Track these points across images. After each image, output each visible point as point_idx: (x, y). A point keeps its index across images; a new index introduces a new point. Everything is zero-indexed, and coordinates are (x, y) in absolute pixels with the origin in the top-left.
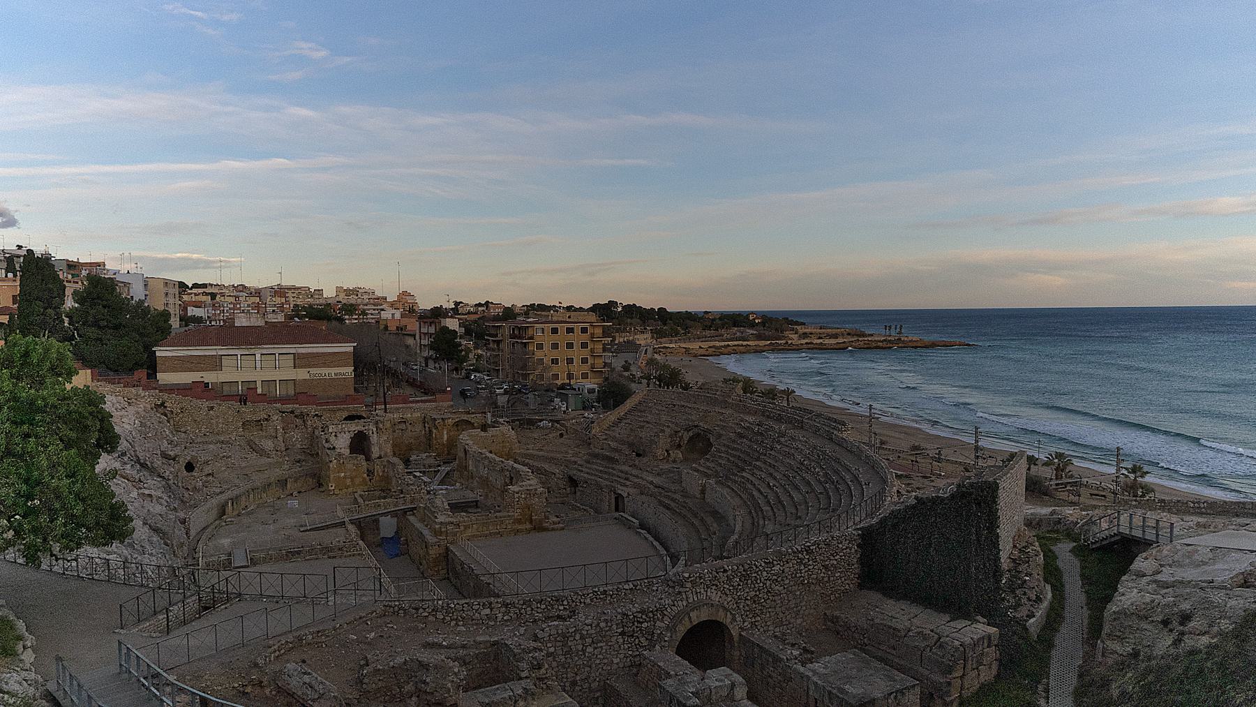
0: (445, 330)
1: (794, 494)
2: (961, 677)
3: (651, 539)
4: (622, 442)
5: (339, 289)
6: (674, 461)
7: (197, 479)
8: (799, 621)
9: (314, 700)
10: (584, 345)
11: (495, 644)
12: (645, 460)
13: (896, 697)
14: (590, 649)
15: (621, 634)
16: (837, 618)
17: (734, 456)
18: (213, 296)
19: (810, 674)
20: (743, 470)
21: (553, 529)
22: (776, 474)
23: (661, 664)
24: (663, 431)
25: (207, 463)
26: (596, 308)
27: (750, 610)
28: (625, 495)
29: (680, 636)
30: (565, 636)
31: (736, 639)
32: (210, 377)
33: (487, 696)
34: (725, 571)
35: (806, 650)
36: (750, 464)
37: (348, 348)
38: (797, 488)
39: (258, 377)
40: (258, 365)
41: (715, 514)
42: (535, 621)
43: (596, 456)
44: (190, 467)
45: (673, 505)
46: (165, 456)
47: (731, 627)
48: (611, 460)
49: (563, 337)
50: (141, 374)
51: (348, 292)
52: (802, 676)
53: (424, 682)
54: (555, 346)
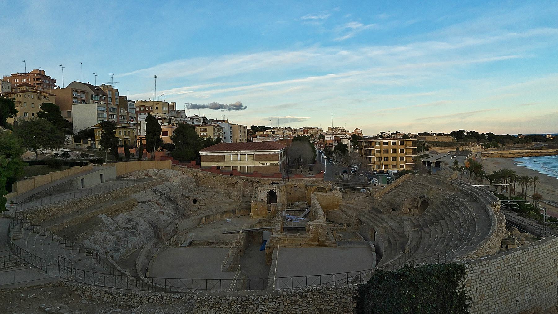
7: (196, 207)
10: (402, 151)
12: (395, 213)
18: (273, 132)
21: (330, 247)
24: (407, 198)
25: (202, 200)
26: (453, 134)
32: (220, 164)
39: (239, 164)
40: (239, 159)
43: (374, 209)
44: (195, 201)
48: (379, 212)
49: (389, 147)
50: (193, 162)
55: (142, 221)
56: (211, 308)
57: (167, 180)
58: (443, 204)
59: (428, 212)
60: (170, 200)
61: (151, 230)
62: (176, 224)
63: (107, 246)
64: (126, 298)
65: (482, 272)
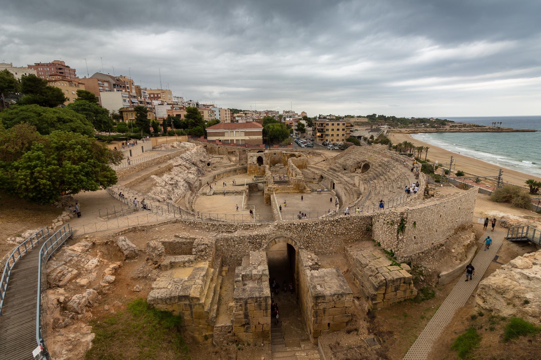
2: (384, 294)
4: (340, 164)
5: (284, 111)
6: (357, 173)
8: (331, 248)
10: (343, 130)
12: (346, 171)
13: (338, 297)
14: (237, 246)
15: (249, 242)
18: (246, 114)
20: (375, 179)
25: (214, 163)
26: (368, 117)
30: (227, 240)
32: (221, 138)
39: (235, 138)
43: (331, 169)
44: (209, 164)
46: (201, 161)
47: (294, 247)
49: (335, 127)
50: (202, 137)
51: (287, 112)
54: (333, 130)
55: (179, 179)
56: (285, 230)
57: (188, 150)
58: (380, 166)
59: (370, 171)
60: (194, 164)
61: (186, 185)
62: (200, 180)
63: (164, 196)
65: (444, 206)
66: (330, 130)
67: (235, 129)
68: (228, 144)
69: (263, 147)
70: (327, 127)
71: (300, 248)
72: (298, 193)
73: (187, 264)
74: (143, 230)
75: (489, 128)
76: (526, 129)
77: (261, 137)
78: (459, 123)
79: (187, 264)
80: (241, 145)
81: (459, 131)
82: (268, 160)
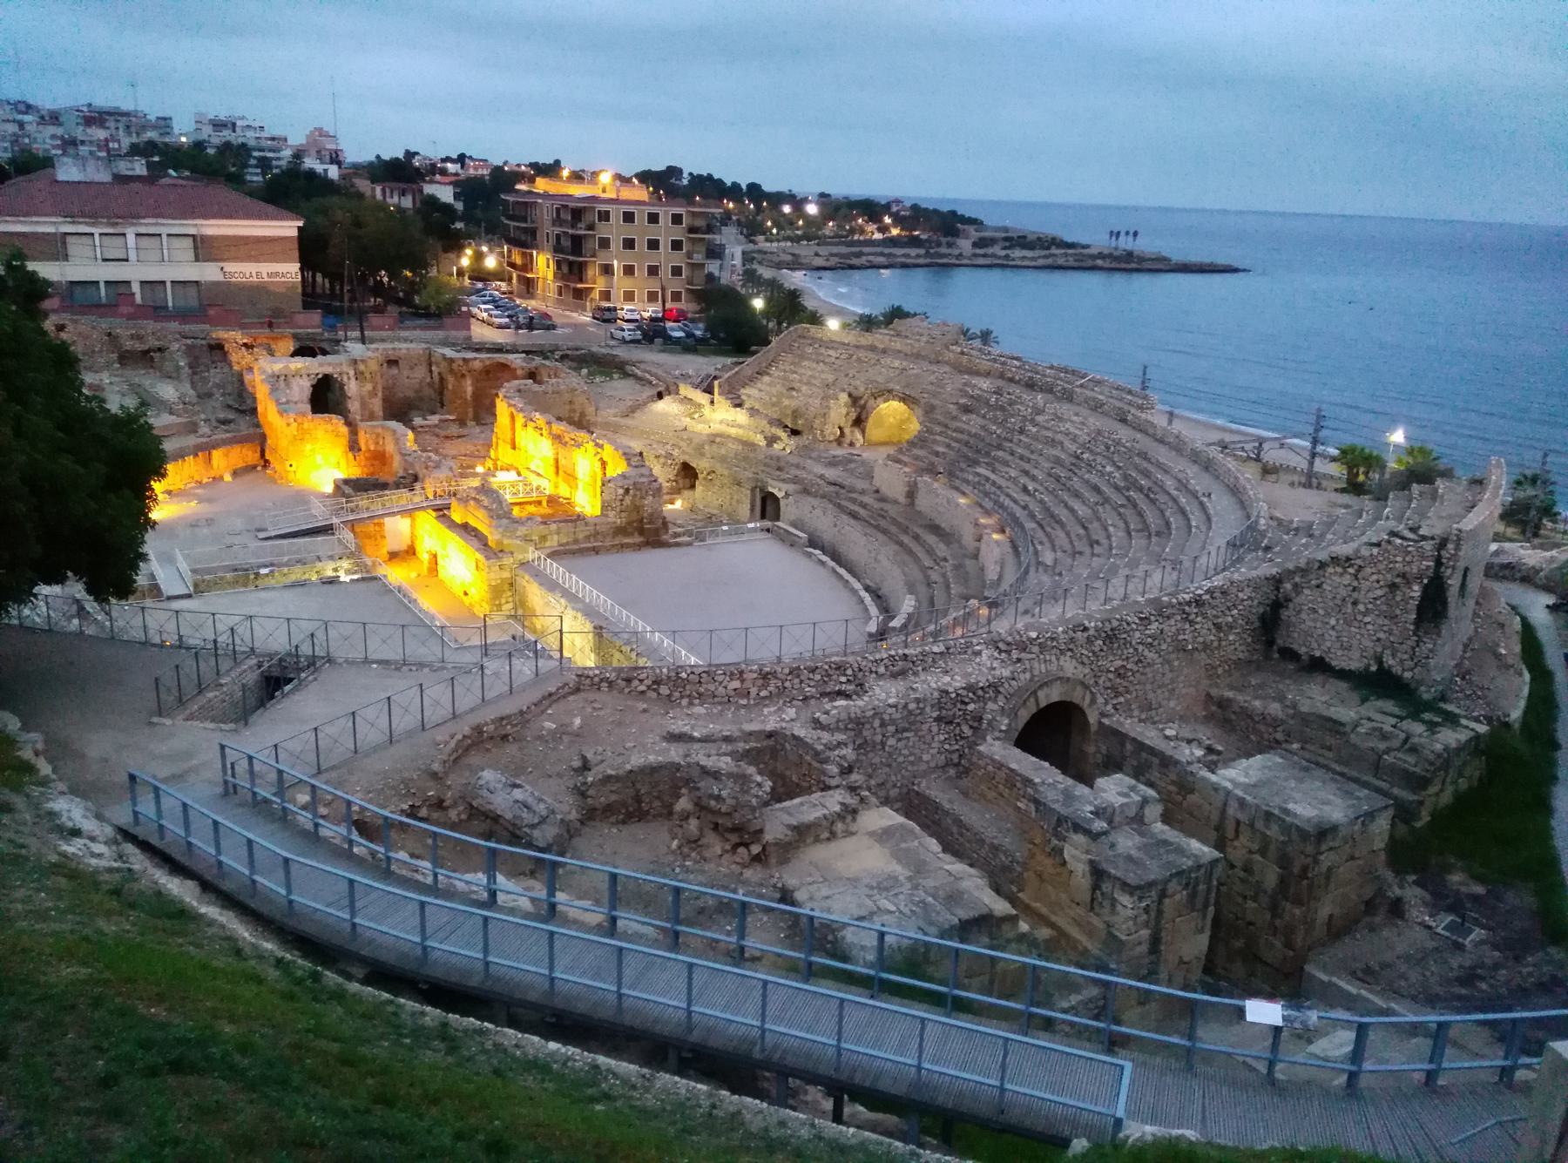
0: (432, 202)
1: (1077, 505)
3: (833, 564)
8: (1172, 704)
9: (533, 826)
10: (677, 245)
11: (770, 735)
14: (891, 742)
15: (938, 719)
16: (1229, 700)
17: (957, 441)
19: (1229, 785)
20: (976, 463)
21: (678, 545)
22: (1035, 472)
23: (1014, 766)
27: (1113, 688)
28: (780, 495)
29: (1021, 724)
31: (1094, 728)
33: (789, 814)
34: (1086, 629)
35: (1210, 750)
36: (988, 454)
37: (288, 228)
38: (1077, 495)
39: (134, 273)
41: (935, 529)
42: (805, 699)
45: (862, 512)
51: (218, 125)
52: (1216, 788)
53: (718, 798)
56: (1062, 652)
64: (818, 677)
66: (616, 245)
67: (133, 216)
68: (96, 308)
69: (312, 324)
70: (603, 230)
71: (1103, 715)
72: (639, 547)
73: (839, 826)
74: (505, 738)
75: (1101, 256)
76: (1207, 260)
77: (289, 271)
78: (997, 229)
79: (839, 826)
80: (183, 315)
81: (1004, 265)
82: (373, 394)
